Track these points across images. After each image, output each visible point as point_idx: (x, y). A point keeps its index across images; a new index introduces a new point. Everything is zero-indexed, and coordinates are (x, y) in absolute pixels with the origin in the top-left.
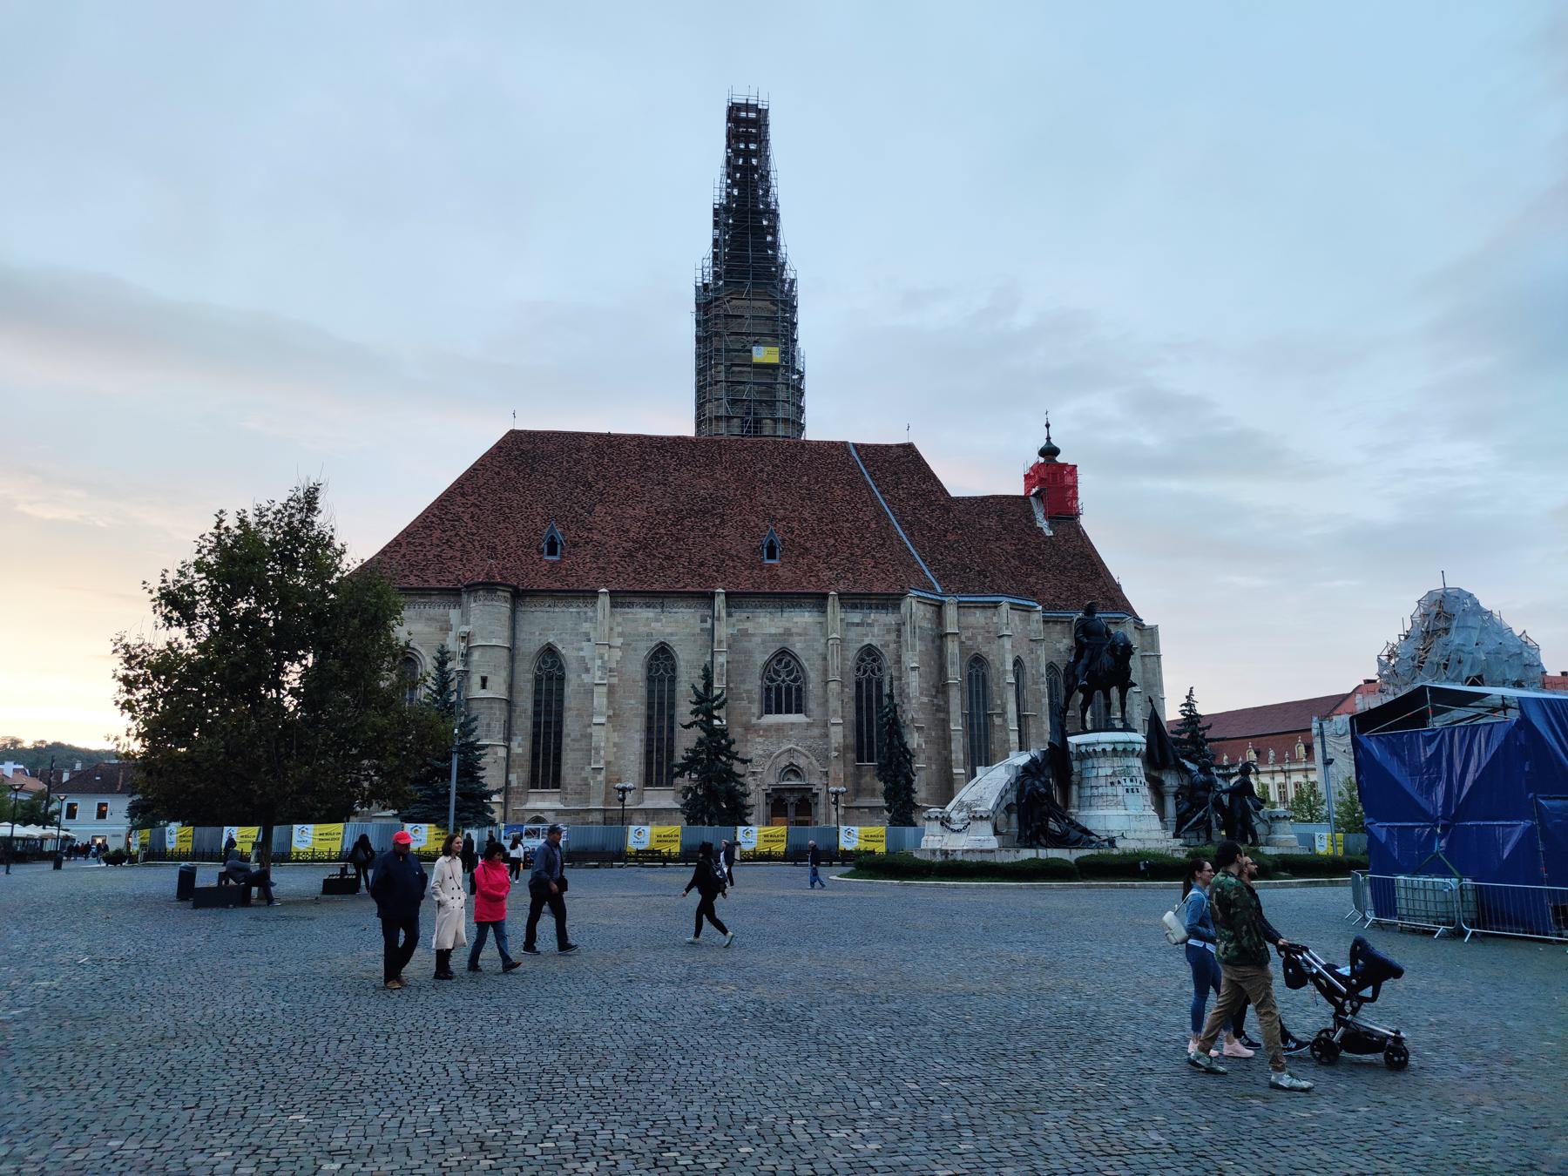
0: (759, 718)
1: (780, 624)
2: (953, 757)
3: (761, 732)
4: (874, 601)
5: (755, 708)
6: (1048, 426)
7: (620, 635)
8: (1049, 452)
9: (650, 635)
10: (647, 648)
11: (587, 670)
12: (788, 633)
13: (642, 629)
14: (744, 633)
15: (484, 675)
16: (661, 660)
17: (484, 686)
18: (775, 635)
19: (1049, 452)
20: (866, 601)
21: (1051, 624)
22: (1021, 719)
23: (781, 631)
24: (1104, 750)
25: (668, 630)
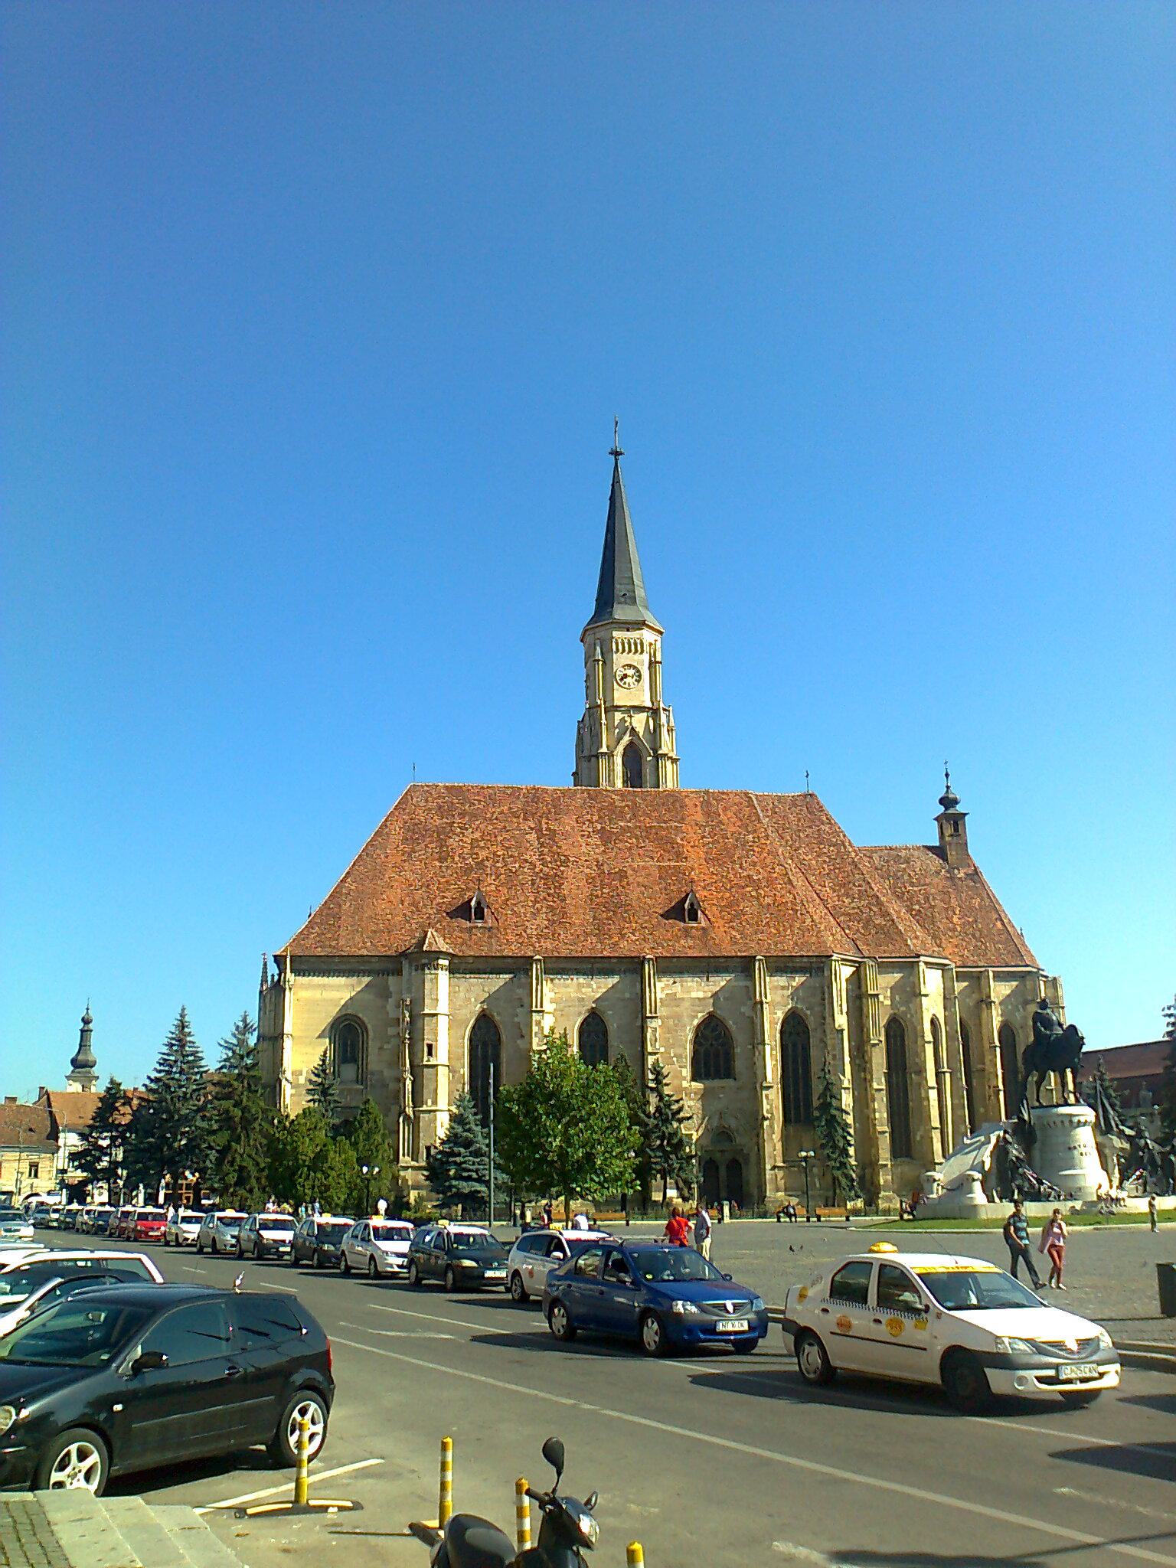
1: (706, 988)
3: (692, 1095)
5: (687, 1072)
6: (947, 775)
8: (947, 802)
11: (522, 1036)
15: (430, 1042)
17: (430, 1054)
19: (947, 802)
22: (939, 1075)
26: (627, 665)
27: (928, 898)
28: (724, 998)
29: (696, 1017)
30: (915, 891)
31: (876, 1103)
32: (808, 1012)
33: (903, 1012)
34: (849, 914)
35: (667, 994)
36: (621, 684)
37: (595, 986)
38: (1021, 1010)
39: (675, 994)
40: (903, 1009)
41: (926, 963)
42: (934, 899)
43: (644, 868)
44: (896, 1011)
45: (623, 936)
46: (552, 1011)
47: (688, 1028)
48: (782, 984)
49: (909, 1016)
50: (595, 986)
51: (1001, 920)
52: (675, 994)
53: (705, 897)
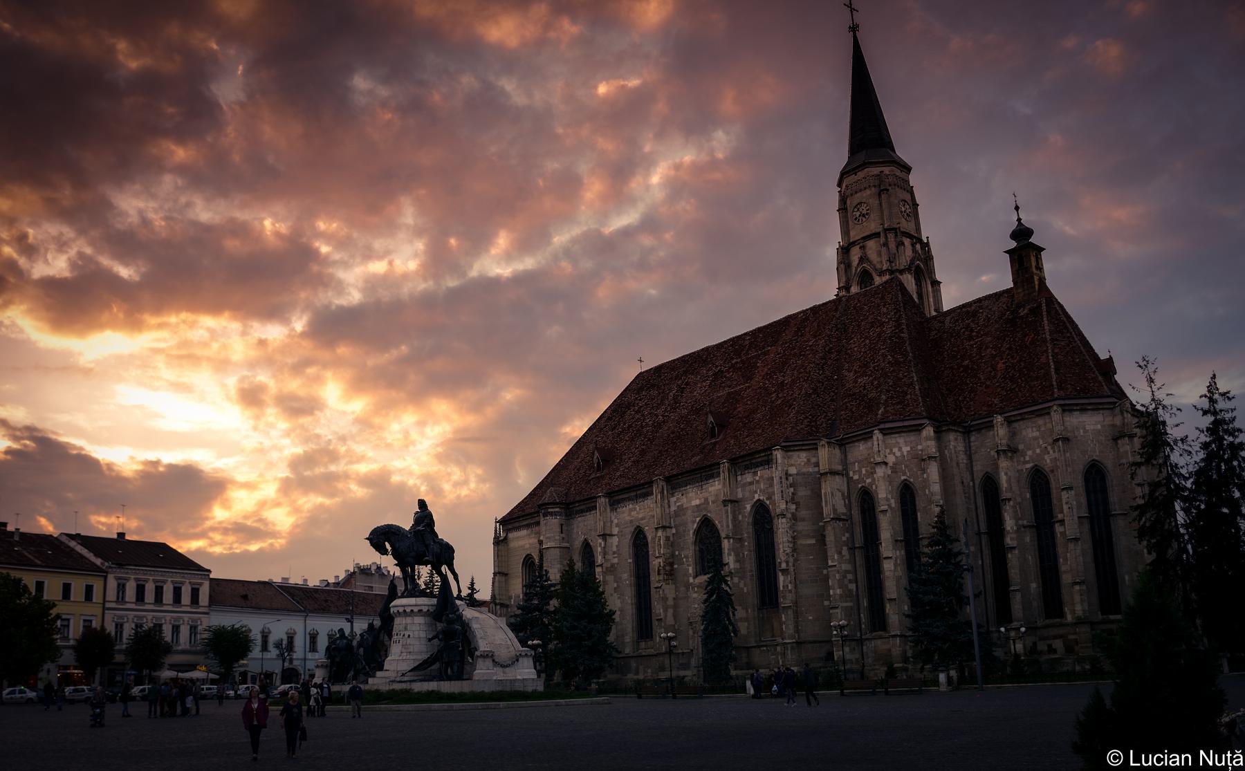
0: (695, 577)
2: (831, 592)
4: (760, 460)
6: (1017, 208)
7: (617, 525)
8: (1022, 234)
9: (631, 521)
10: (631, 532)
12: (706, 499)
13: (628, 518)
14: (681, 508)
16: (639, 540)
18: (700, 505)
19: (1022, 234)
20: (754, 461)
21: (983, 431)
23: (703, 500)
24: (412, 611)
25: (640, 516)
26: (858, 204)
27: (981, 348)
28: (713, 502)
29: (694, 522)
30: (972, 346)
31: (830, 581)
32: (768, 502)
33: (869, 484)
34: (854, 394)
35: (678, 506)
36: (856, 222)
37: (638, 509)
38: (1051, 452)
39: (682, 505)
40: (869, 481)
41: (879, 429)
42: (987, 348)
43: (719, 397)
44: (864, 484)
45: (664, 462)
46: (616, 533)
47: (691, 532)
48: (749, 480)
49: (874, 487)
50: (638, 509)
51: (1047, 353)
52: (682, 505)
53: (739, 412)
